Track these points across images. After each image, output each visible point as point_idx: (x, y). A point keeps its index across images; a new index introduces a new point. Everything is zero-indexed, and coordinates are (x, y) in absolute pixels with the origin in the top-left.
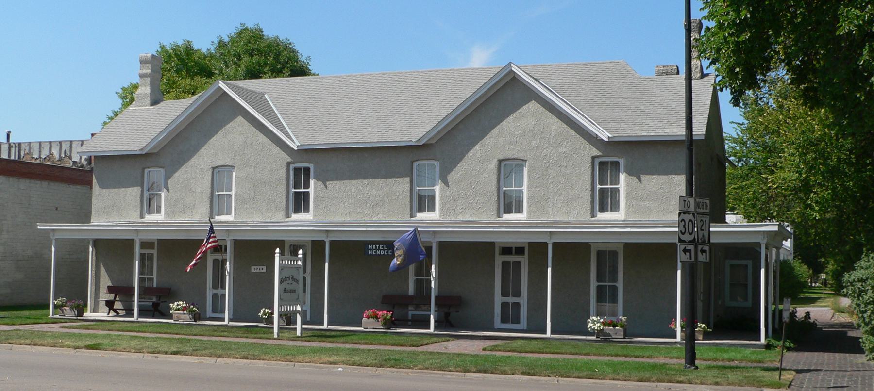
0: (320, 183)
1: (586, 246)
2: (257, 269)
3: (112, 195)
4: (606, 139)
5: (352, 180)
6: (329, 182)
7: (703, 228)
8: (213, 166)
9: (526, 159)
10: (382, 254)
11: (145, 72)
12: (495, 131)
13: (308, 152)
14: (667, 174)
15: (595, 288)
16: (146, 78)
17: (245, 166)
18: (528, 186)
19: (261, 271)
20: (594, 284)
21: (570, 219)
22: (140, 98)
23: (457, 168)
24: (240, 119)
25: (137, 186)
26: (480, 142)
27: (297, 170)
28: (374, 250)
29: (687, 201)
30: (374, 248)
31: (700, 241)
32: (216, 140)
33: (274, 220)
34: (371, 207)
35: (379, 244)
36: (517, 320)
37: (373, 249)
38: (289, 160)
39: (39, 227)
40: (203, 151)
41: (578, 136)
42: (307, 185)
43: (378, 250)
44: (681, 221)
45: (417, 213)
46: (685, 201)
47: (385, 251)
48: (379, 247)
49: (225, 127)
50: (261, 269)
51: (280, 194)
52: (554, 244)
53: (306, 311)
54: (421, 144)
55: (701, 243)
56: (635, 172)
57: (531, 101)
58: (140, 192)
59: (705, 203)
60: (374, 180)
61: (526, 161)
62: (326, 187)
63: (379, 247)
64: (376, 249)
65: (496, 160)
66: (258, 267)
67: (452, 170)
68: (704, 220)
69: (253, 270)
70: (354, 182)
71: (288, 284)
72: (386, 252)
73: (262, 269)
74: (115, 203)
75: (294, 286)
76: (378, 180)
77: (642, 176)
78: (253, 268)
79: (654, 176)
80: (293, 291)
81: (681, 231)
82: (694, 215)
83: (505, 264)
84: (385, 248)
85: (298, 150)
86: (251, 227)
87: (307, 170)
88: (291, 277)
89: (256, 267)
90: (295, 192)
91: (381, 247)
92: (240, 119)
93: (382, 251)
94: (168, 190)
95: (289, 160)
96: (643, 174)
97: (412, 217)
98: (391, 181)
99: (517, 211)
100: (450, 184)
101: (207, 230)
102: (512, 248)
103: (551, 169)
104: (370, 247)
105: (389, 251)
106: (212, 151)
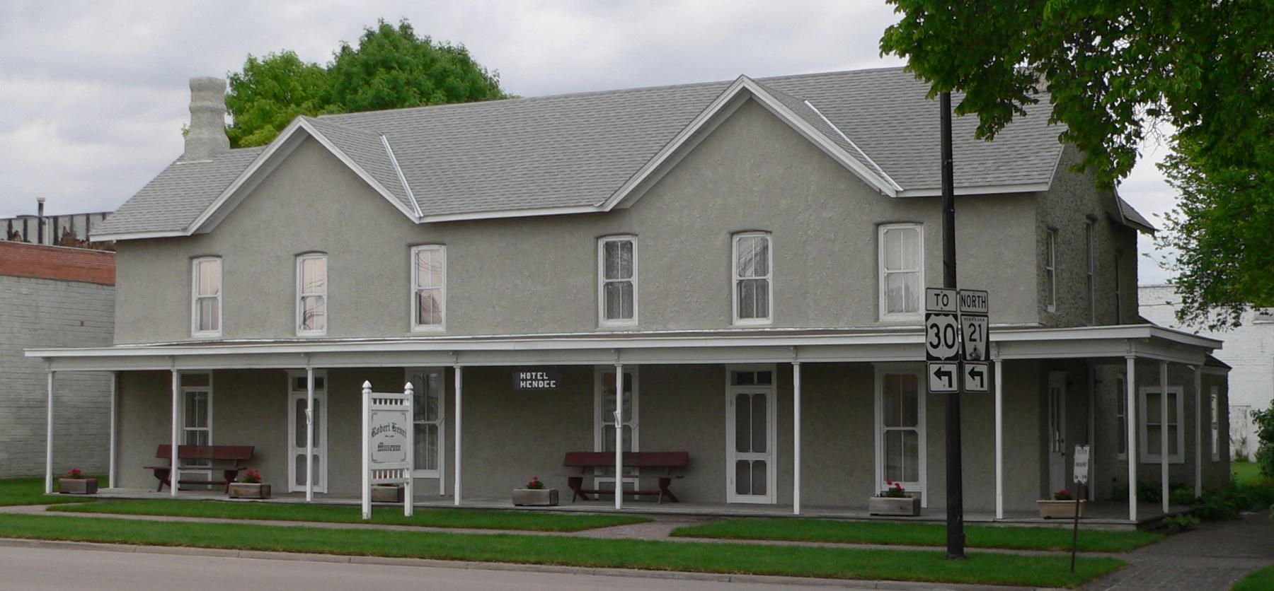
4: (893, 195)
7: (976, 336)
8: (298, 252)
10: (540, 386)
15: (882, 435)
18: (774, 273)
28: (529, 380)
29: (942, 295)
30: (528, 378)
31: (968, 358)
37: (527, 380)
39: (27, 354)
43: (535, 380)
44: (931, 327)
46: (937, 295)
47: (546, 382)
48: (536, 376)
53: (439, 479)
54: (608, 209)
55: (971, 360)
59: (979, 297)
63: (536, 376)
64: (531, 379)
65: (725, 232)
68: (976, 324)
71: (387, 436)
72: (548, 384)
75: (397, 439)
80: (396, 448)
81: (931, 343)
82: (955, 317)
83: (742, 400)
84: (545, 378)
88: (391, 425)
91: (539, 375)
93: (540, 382)
99: (760, 314)
102: (752, 373)
104: (522, 376)
105: (552, 382)
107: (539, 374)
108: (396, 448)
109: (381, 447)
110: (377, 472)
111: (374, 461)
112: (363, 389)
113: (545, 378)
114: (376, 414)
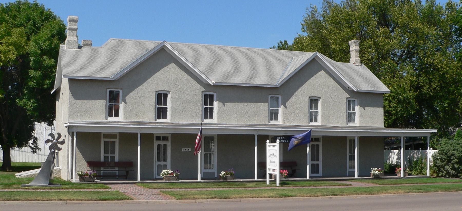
0: (221, 104)
1: (345, 137)
2: (185, 150)
3: (84, 104)
5: (239, 102)
8: (157, 90)
10: (283, 141)
12: (307, 83)
14: (374, 107)
16: (73, 31)
17: (177, 91)
19: (188, 151)
20: (348, 154)
21: (339, 125)
22: (70, 43)
23: (290, 99)
24: (173, 65)
25: (104, 99)
26: (301, 88)
27: (206, 96)
32: (157, 75)
33: (195, 123)
34: (249, 117)
36: (318, 172)
38: (203, 90)
40: (150, 80)
41: (341, 88)
42: (212, 104)
45: (271, 121)
47: (285, 140)
48: (282, 138)
49: (164, 68)
50: (188, 150)
51: (199, 108)
53: (215, 172)
56: (363, 105)
57: (322, 70)
58: (105, 103)
60: (250, 103)
62: (224, 105)
63: (282, 138)
66: (186, 149)
67: (288, 100)
69: (183, 150)
72: (286, 141)
73: (189, 150)
74: (86, 110)
76: (252, 103)
77: (365, 107)
78: (183, 149)
79: (369, 108)
84: (285, 139)
86: (339, 130)
87: (212, 96)
89: (185, 149)
90: (205, 108)
92: (322, 73)
93: (283, 140)
94: (126, 103)
95: (203, 90)
96: (366, 106)
97: (269, 123)
98: (259, 104)
99: (315, 121)
100: (287, 107)
101: (200, 128)
103: (331, 102)
105: (287, 140)
106: (156, 82)
107: (283, 138)
113: (285, 139)
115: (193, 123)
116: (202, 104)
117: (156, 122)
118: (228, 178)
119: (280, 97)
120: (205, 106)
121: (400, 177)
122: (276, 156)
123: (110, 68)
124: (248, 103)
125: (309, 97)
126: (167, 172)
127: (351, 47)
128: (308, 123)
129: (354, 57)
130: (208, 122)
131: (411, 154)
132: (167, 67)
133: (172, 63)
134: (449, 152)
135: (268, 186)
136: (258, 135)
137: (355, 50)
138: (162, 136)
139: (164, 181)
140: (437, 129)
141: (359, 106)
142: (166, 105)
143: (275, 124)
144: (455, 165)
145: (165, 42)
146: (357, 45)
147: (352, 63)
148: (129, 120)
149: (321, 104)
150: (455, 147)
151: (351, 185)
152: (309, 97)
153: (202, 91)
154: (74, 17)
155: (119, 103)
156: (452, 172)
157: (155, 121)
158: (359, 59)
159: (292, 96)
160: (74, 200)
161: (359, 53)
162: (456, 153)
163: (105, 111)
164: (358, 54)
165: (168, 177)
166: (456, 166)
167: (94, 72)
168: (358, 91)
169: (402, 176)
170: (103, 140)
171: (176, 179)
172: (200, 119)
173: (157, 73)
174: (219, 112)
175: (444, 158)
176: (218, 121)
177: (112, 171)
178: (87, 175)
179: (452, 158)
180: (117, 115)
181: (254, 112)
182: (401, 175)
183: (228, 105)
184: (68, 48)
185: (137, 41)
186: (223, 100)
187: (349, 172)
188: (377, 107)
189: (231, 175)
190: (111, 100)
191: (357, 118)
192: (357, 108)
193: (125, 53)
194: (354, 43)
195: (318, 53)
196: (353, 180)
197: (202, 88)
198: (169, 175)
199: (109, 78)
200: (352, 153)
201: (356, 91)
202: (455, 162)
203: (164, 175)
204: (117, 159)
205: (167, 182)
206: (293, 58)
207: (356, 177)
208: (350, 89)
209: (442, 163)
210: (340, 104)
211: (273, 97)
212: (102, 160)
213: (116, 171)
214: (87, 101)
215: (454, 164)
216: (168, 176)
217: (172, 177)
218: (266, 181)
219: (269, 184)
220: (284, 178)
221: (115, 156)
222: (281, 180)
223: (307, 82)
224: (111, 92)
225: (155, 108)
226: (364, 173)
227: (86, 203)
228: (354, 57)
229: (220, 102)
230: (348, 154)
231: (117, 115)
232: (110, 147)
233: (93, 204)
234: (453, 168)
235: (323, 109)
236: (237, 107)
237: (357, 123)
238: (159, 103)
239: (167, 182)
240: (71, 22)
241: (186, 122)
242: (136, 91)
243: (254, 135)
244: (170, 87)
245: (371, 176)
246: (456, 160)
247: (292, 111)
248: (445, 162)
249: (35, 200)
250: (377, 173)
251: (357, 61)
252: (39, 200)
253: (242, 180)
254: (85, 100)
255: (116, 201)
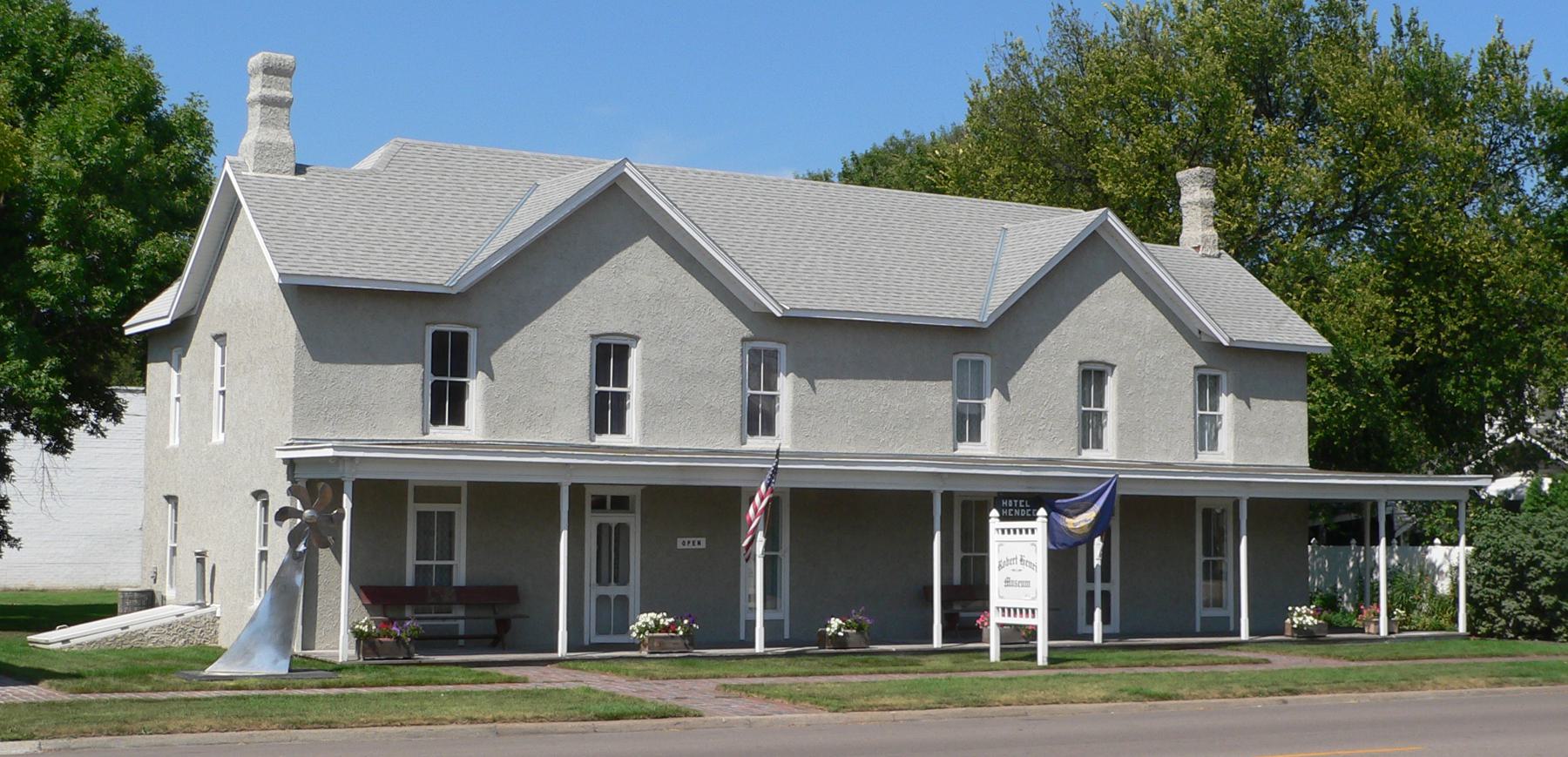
0: (804, 382)
2: (689, 542)
5: (859, 379)
6: (819, 381)
8: (595, 333)
9: (1115, 363)
11: (279, 95)
12: (1074, 316)
13: (800, 325)
16: (279, 109)
17: (661, 337)
19: (697, 546)
20: (1200, 559)
23: (1022, 369)
24: (647, 243)
27: (754, 353)
32: (597, 279)
33: (719, 448)
34: (891, 429)
35: (1019, 499)
37: (1008, 508)
38: (747, 333)
41: (1178, 334)
42: (771, 385)
48: (1018, 503)
50: (696, 543)
52: (1251, 501)
56: (1244, 394)
57: (1118, 272)
61: (1115, 366)
62: (814, 389)
63: (1018, 503)
64: (1013, 507)
66: (691, 540)
69: (680, 546)
70: (862, 383)
71: (1014, 570)
72: (1030, 513)
73: (699, 543)
74: (356, 398)
77: (1252, 400)
78: (680, 541)
80: (1026, 584)
84: (1027, 506)
85: (782, 317)
88: (1019, 558)
89: (686, 540)
95: (747, 333)
98: (924, 385)
100: (1011, 397)
101: (770, 469)
107: (1021, 501)
108: (1026, 584)
109: (1008, 582)
110: (1006, 610)
111: (1001, 597)
112: (990, 518)
113: (1027, 506)
114: (1001, 545)
115: (715, 448)
116: (742, 383)
117: (593, 444)
118: (851, 639)
119: (988, 361)
120: (750, 391)
121: (1377, 636)
122: (1033, 566)
123: (432, 249)
124: (890, 382)
125: (1081, 363)
126: (657, 622)
127: (1186, 193)
128: (1076, 450)
129: (1197, 226)
130: (762, 446)
131: (1360, 557)
132: (629, 249)
133: (645, 236)
134: (1521, 554)
135: (993, 668)
136: (945, 491)
137: (1202, 204)
138: (609, 493)
139: (644, 653)
140: (1492, 476)
141: (1231, 396)
142: (625, 385)
143: (974, 453)
144: (1540, 596)
145: (628, 164)
146: (1206, 186)
147: (1189, 248)
148: (502, 437)
149: (1115, 388)
150: (1543, 536)
151: (1267, 662)
152: (1081, 363)
153: (741, 336)
154: (279, 56)
155: (465, 376)
156: (1531, 620)
157: (589, 443)
158: (1213, 232)
159: (1026, 359)
160: (514, 720)
161: (1212, 214)
162: (1548, 558)
163: (420, 404)
164: (1209, 216)
165: (659, 641)
166: (1547, 600)
167: (382, 265)
168: (1232, 345)
169: (1383, 632)
170: (413, 508)
171: (685, 644)
172: (735, 435)
173: (598, 271)
174: (797, 411)
175: (1499, 574)
176: (795, 442)
177: (444, 619)
178: (390, 637)
179: (1530, 575)
180: (458, 418)
181: (907, 413)
182: (1379, 629)
183: (826, 387)
184: (261, 170)
185: (488, 152)
186: (810, 371)
187: (1203, 619)
188: (1288, 400)
189: (860, 629)
190: (438, 367)
191: (1225, 437)
192: (1226, 403)
193: (463, 195)
194: (1199, 179)
195: (1110, 213)
196: (1240, 648)
197: (744, 327)
198: (660, 632)
199: (441, 285)
200: (1210, 556)
201: (1226, 344)
202: (1544, 587)
203: (647, 633)
204: (460, 578)
205: (658, 655)
206: (1005, 226)
207: (1244, 635)
208: (1204, 339)
209: (1493, 591)
210: (1176, 386)
211: (967, 361)
212: (410, 580)
213: (458, 620)
214: (358, 367)
215: (1539, 592)
216: (658, 634)
217: (672, 637)
218: (987, 650)
219: (998, 660)
220: (1024, 641)
221: (454, 567)
222: (1004, 646)
223: (1072, 312)
224: (439, 337)
225: (590, 395)
226: (1268, 623)
227: (560, 730)
228: (1197, 226)
229: (799, 377)
230: (1200, 559)
231: (458, 418)
232: (436, 533)
233: (583, 733)
234: (1536, 609)
235: (1121, 408)
236: (852, 394)
237: (1225, 452)
238: (601, 378)
239: (658, 655)
240: (271, 77)
241: (691, 447)
242: (526, 333)
243: (929, 491)
244: (640, 323)
245: (1288, 632)
246: (1544, 581)
247: (1028, 410)
248: (1503, 585)
249: (390, 723)
250: (1310, 624)
251: (1207, 241)
252: (402, 725)
253: (893, 648)
254: (352, 364)
255: (649, 722)
